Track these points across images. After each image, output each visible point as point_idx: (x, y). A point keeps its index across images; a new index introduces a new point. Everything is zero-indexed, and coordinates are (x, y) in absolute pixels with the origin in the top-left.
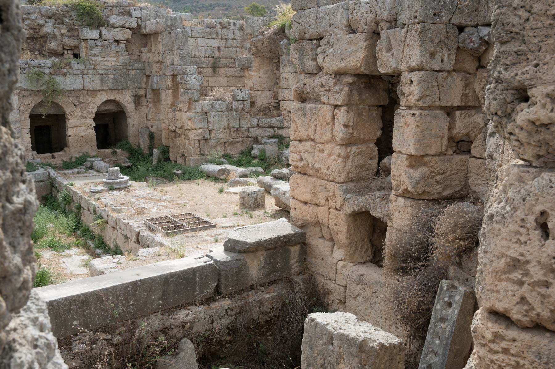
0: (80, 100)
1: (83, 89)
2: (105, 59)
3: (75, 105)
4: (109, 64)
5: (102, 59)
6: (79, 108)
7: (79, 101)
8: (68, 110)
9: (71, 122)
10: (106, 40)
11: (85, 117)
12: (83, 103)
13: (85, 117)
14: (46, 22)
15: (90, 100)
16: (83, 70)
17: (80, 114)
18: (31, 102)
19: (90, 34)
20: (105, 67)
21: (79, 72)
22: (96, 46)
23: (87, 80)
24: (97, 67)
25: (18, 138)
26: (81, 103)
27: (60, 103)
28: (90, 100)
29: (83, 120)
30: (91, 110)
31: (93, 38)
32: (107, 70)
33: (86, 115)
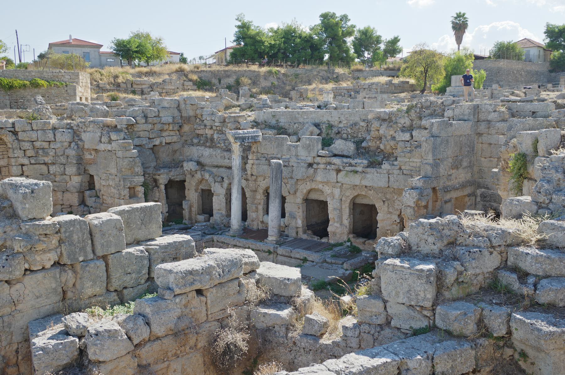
0: (387, 196)
1: (389, 187)
2: (411, 160)
3: (384, 201)
4: (414, 165)
5: (408, 160)
6: (386, 204)
7: (386, 198)
11: (390, 213)
13: (390, 213)
15: (396, 197)
16: (389, 170)
17: (386, 209)
18: (350, 194)
20: (410, 168)
21: (385, 172)
23: (392, 179)
24: (403, 168)
25: (337, 222)
26: (388, 200)
28: (396, 197)
29: (389, 216)
30: (396, 207)
32: (411, 170)
33: (391, 210)
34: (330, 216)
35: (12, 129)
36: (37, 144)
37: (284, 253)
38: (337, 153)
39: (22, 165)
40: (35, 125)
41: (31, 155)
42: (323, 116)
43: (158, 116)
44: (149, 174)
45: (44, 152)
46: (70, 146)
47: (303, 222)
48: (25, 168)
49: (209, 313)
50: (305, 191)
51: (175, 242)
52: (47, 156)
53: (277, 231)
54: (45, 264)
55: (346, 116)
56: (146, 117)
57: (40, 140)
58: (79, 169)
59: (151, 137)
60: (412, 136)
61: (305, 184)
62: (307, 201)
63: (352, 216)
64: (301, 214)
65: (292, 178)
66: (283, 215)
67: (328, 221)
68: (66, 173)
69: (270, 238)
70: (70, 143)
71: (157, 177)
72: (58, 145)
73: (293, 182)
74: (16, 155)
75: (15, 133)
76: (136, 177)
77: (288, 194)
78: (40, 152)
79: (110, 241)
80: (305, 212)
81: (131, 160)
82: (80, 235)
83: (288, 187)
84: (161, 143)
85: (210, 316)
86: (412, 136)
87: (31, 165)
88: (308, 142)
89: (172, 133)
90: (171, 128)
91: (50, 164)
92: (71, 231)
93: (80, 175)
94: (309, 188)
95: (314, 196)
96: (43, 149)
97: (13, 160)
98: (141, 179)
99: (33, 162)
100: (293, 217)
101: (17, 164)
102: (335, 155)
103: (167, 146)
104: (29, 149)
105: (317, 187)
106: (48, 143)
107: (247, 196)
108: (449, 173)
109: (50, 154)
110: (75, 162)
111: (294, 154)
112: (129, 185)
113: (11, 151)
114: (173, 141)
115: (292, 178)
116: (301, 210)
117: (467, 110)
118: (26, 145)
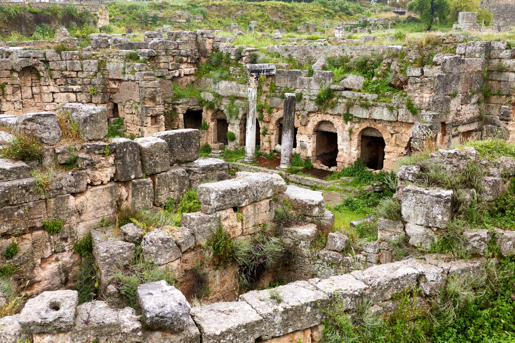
0: (396, 130)
1: (397, 120)
3: (392, 134)
6: (394, 136)
8: (386, 137)
9: (387, 148)
10: (427, 77)
11: (398, 145)
12: (398, 133)
14: (393, 61)
17: (394, 142)
19: (412, 72)
22: (416, 83)
27: (380, 130)
28: (403, 131)
29: (396, 147)
30: (404, 140)
31: (414, 75)
33: (398, 143)
34: (339, 147)
35: (44, 59)
36: (66, 73)
37: (295, 180)
38: (347, 87)
39: (53, 93)
40: (64, 55)
41: (60, 84)
42: (335, 52)
43: (177, 48)
44: (169, 104)
45: (72, 81)
46: (96, 76)
47: (313, 152)
48: (55, 96)
49: (244, 228)
50: (316, 123)
51: (211, 165)
52: (75, 85)
53: (289, 159)
54: (103, 180)
55: (358, 51)
56: (166, 50)
57: (68, 69)
58: (104, 97)
59: (171, 69)
60: (422, 72)
61: (316, 116)
62: (317, 131)
63: (360, 147)
64: (311, 144)
65: (303, 110)
66: (295, 146)
67: (336, 151)
68: (93, 101)
69: (282, 166)
70: (96, 73)
71: (177, 106)
72: (85, 74)
73: (305, 113)
74: (47, 84)
75: (46, 62)
76: (158, 106)
77: (300, 125)
78: (69, 81)
79: (157, 162)
80: (315, 143)
81: (153, 90)
82: (132, 155)
83: (300, 119)
84: (180, 74)
85: (245, 231)
86: (422, 72)
87: (61, 93)
88: (321, 76)
89: (189, 66)
90: (189, 61)
91: (78, 92)
92: (124, 152)
93: (105, 103)
94: (320, 120)
95: (325, 128)
96: (72, 77)
97: (45, 88)
98: (161, 109)
99: (62, 90)
100: (304, 148)
101: (48, 92)
102: (346, 89)
103: (186, 77)
104: (58, 78)
105: (327, 120)
106: (76, 73)
107: (260, 126)
108: (458, 109)
109: (78, 83)
110: (101, 91)
111: (307, 87)
112: (151, 113)
113: (42, 79)
114: (191, 73)
115: (303, 110)
116: (311, 141)
117: (480, 48)
118: (56, 75)
